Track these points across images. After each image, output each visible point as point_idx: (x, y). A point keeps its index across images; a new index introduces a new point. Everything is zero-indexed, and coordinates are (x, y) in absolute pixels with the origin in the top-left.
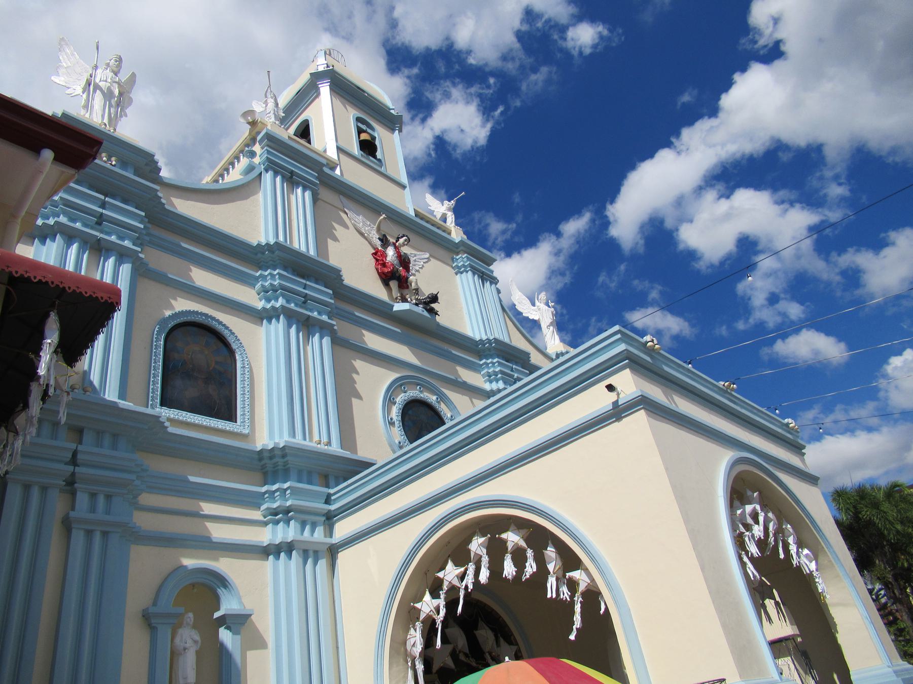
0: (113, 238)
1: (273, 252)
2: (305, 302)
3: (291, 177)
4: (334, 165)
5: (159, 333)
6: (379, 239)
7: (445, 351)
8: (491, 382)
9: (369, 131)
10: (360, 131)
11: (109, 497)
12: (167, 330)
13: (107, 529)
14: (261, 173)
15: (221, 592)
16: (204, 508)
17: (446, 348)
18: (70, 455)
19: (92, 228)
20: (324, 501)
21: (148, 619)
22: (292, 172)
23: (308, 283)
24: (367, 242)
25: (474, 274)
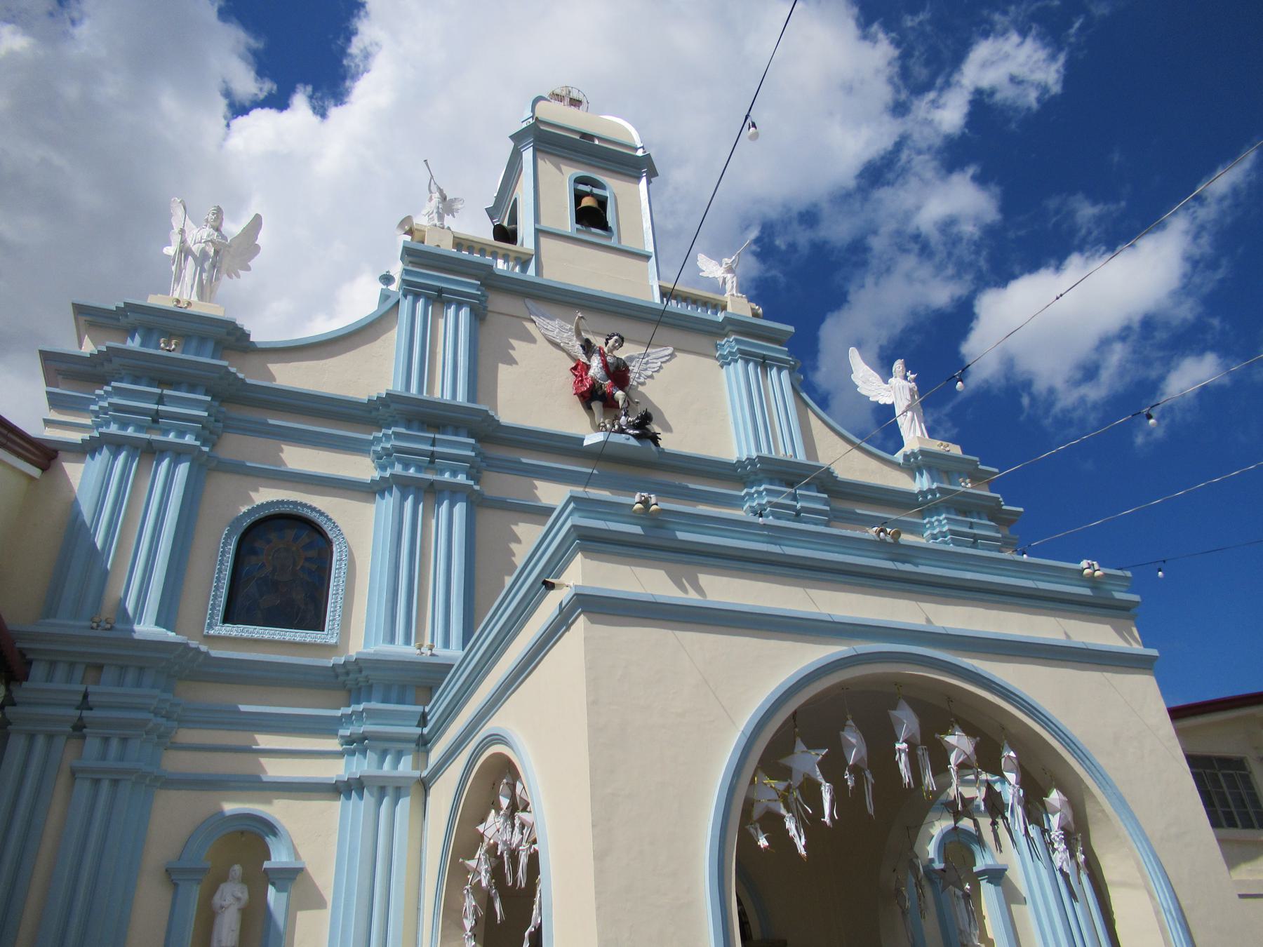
0: (171, 437)
1: (387, 406)
2: (432, 462)
3: (440, 296)
4: (526, 257)
5: (228, 536)
6: (581, 346)
7: (676, 486)
9: (596, 191)
10: (578, 197)
11: (124, 740)
12: (241, 530)
13: (98, 776)
14: (398, 301)
15: (271, 841)
16: (259, 741)
17: (677, 483)
18: (80, 698)
19: (147, 429)
20: (416, 723)
21: (173, 876)
22: (440, 291)
23: (438, 436)
24: (565, 354)
25: (747, 362)
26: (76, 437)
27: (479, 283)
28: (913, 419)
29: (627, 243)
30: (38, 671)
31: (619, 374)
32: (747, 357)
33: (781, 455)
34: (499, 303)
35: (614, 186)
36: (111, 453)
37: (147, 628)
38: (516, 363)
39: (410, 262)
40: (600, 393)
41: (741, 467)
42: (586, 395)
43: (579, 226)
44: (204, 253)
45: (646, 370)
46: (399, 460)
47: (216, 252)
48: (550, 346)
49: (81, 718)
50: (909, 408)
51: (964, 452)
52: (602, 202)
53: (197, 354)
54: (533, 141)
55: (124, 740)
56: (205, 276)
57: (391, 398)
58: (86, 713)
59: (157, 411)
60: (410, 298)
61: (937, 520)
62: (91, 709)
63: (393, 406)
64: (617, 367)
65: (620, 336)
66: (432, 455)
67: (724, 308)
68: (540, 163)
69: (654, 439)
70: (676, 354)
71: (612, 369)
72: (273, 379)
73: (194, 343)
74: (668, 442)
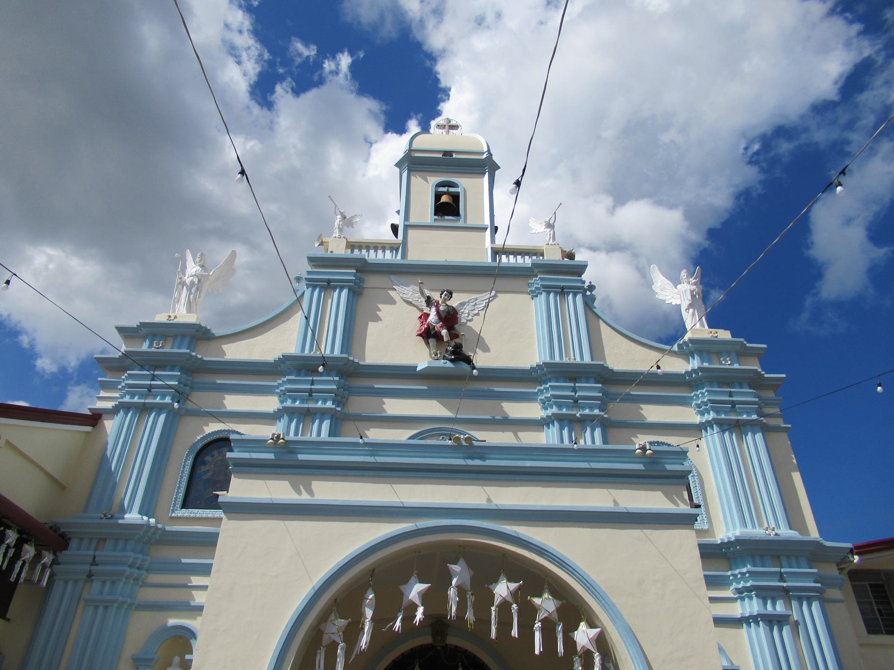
1: (284, 363)
2: (310, 395)
4: (397, 246)
5: (188, 455)
8: (546, 409)
9: (451, 190)
10: (438, 196)
11: (113, 582)
12: (196, 451)
14: (304, 292)
16: (193, 581)
17: (486, 388)
18: (91, 559)
22: (329, 281)
23: (314, 378)
24: (415, 308)
25: (548, 293)
26: (109, 405)
27: (355, 271)
28: (693, 314)
29: (471, 222)
30: (73, 544)
31: (450, 318)
32: (548, 289)
33: (572, 361)
34: (372, 281)
35: (465, 184)
36: (124, 413)
37: (133, 516)
38: (381, 320)
39: (313, 266)
40: (432, 333)
41: (534, 372)
42: (424, 335)
43: (436, 217)
44: (192, 283)
45: (474, 310)
46: (290, 397)
47: (199, 281)
48: (406, 304)
49: (90, 571)
50: (690, 306)
51: (733, 336)
52: (456, 197)
53: (179, 348)
54: (407, 166)
55: (113, 582)
56: (192, 296)
57: (286, 358)
58: (93, 568)
59: (150, 385)
60: (310, 289)
61: (700, 393)
62: (97, 565)
63: (288, 363)
64: (448, 312)
65: (448, 291)
66: (311, 392)
67: (542, 255)
68: (413, 178)
69: (468, 361)
70: (498, 295)
71: (443, 315)
72: (224, 354)
73: (178, 340)
74: (481, 360)
